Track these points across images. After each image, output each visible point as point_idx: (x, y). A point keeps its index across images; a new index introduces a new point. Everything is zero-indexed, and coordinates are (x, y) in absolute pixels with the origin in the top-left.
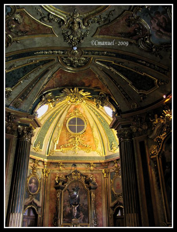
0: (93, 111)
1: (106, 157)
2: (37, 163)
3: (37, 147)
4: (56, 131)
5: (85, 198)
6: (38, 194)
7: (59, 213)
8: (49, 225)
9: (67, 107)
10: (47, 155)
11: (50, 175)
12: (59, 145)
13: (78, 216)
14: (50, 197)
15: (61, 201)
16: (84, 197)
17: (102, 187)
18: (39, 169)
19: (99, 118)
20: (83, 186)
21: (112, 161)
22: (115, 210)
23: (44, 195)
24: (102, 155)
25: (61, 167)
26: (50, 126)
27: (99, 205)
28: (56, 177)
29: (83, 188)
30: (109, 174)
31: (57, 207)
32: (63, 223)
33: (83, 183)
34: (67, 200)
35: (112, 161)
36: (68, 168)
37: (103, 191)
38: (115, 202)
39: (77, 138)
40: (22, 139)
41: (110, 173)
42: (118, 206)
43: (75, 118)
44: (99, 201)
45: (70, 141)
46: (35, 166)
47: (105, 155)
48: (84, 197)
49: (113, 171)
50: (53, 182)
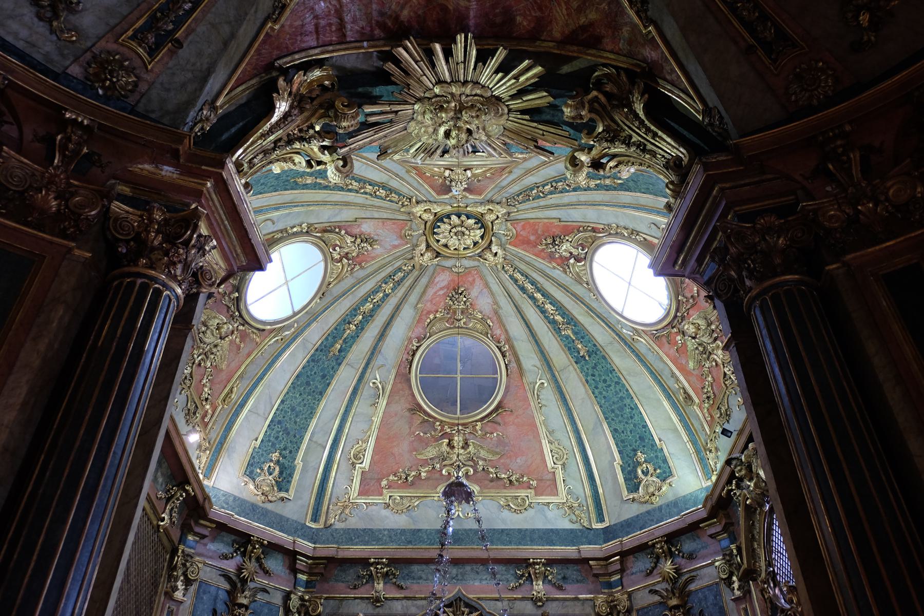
1: (609, 534)
2: (258, 559)
4: (361, 406)
9: (411, 287)
18: (265, 591)
19: (567, 337)
21: (642, 548)
25: (380, 586)
26: (332, 377)
36: (415, 587)
45: (431, 452)
46: (245, 573)
47: (601, 519)
49: (657, 598)
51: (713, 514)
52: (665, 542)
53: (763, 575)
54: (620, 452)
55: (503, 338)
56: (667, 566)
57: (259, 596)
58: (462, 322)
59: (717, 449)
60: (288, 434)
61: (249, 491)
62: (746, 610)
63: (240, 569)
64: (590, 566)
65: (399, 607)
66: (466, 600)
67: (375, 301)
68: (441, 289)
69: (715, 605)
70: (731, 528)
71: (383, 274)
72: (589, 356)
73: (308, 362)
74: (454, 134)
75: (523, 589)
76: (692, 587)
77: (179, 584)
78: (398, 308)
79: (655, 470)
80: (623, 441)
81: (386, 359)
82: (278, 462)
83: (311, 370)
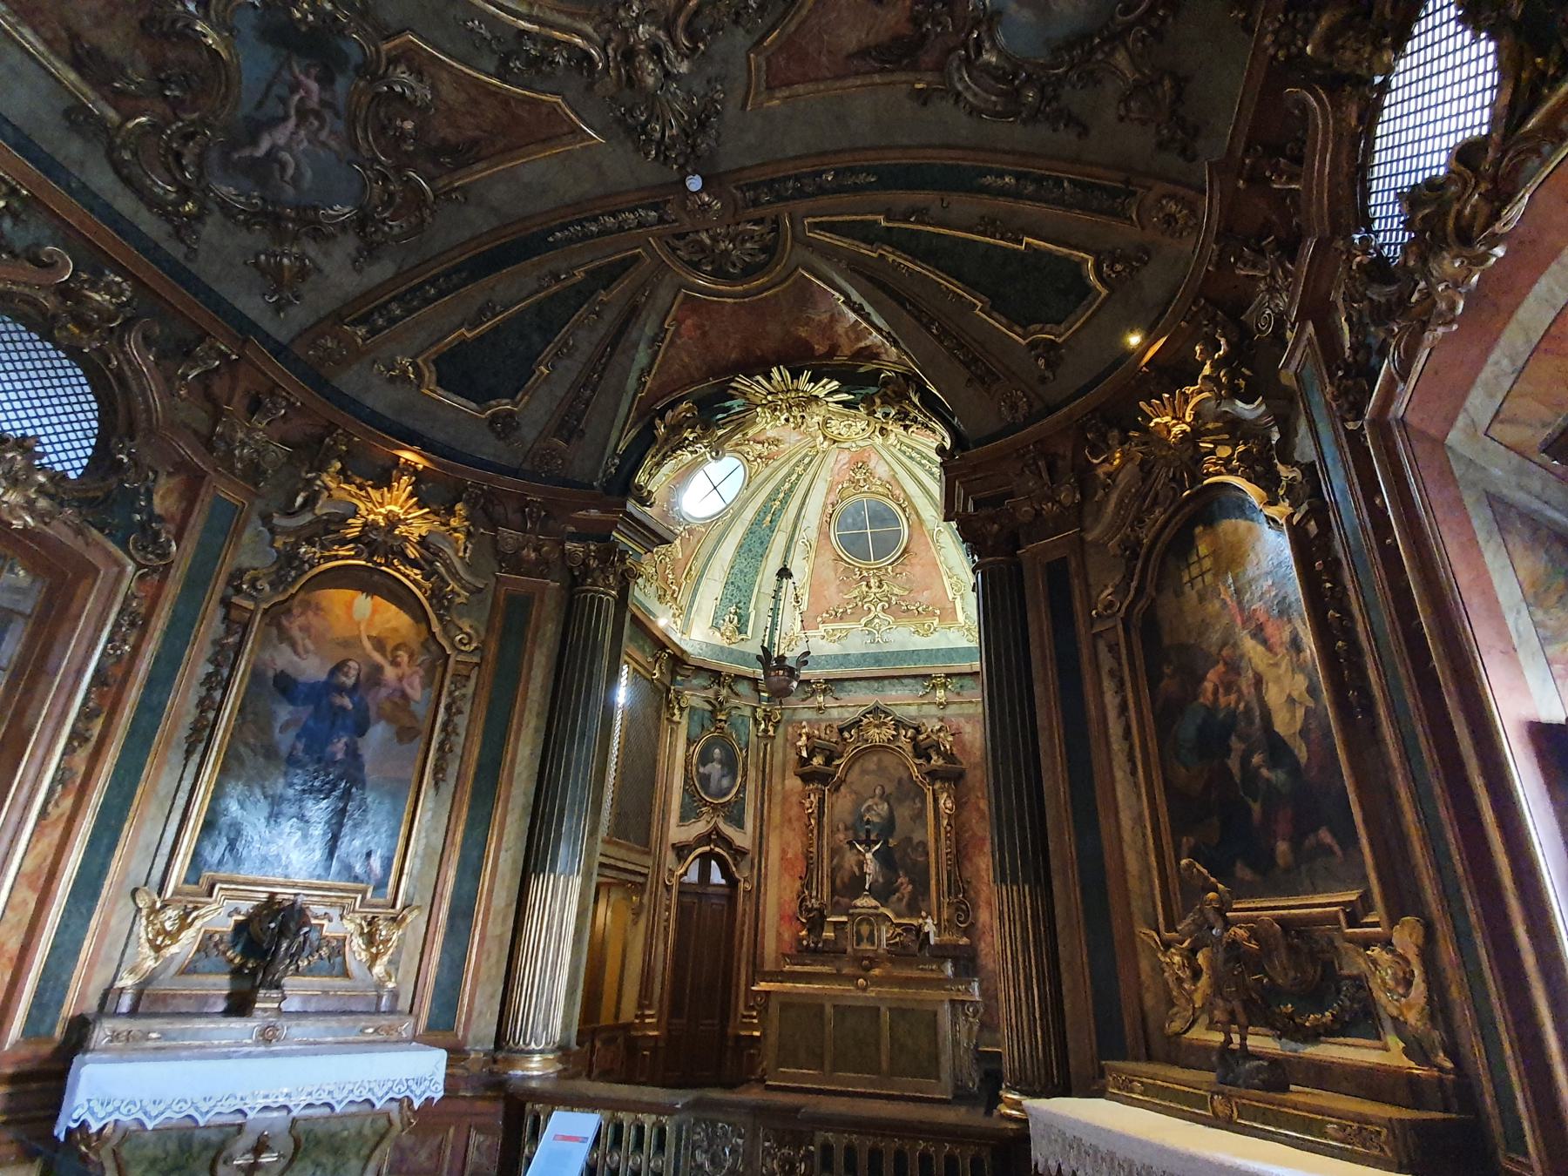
2: (730, 687)
11: (781, 729)
28: (800, 735)
29: (905, 776)
40: (583, 591)
46: (721, 698)
61: (717, 639)
63: (717, 694)
71: (794, 461)
74: (791, 420)
75: (929, 696)
77: (676, 711)
82: (736, 613)
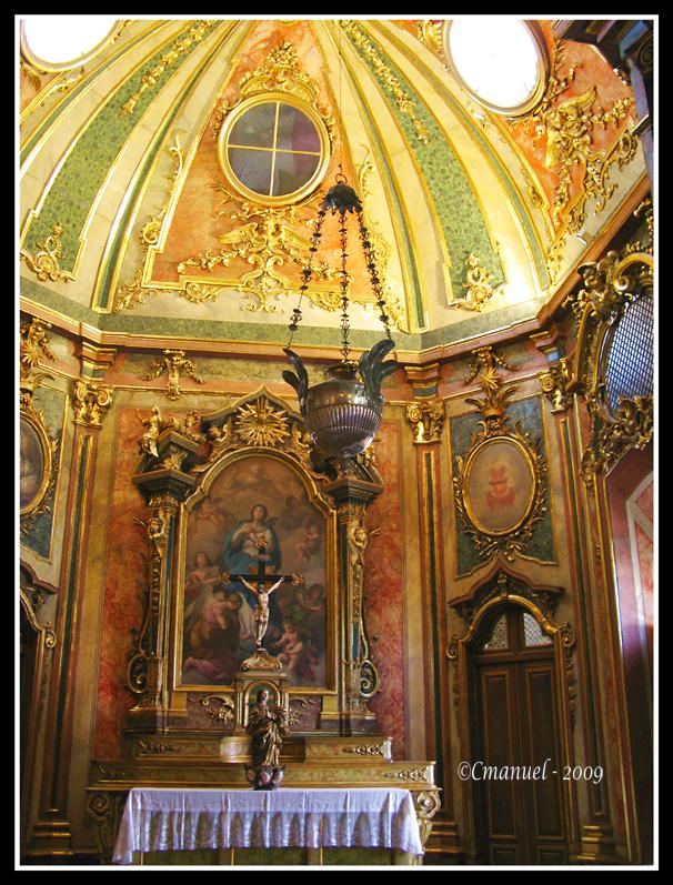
0: (374, 67)
1: (427, 339)
3: (43, 253)
5: (312, 551)
6: (39, 516)
7: (161, 625)
8: (101, 689)
10: (99, 310)
11: (110, 418)
12: (172, 260)
13: (272, 646)
14: (109, 538)
15: (175, 560)
16: (303, 545)
17: (401, 497)
18: (49, 377)
20: (301, 483)
22: (477, 616)
23: (77, 525)
24: (404, 328)
25: (175, 379)
27: (384, 595)
28: (148, 425)
29: (297, 494)
30: (441, 427)
31: (147, 594)
32: (184, 682)
33: (296, 466)
34: (207, 557)
35: (466, 357)
37: (407, 518)
38: (482, 573)
39: (270, 224)
41: (448, 422)
42: (498, 599)
43: (267, 110)
44: (389, 571)
45: (234, 236)
47: (422, 325)
48: (307, 540)
49: (473, 408)
50: (129, 456)
51: (546, 325)
52: (490, 351)
53: (593, 389)
54: (450, 253)
55: (330, 109)
56: (489, 376)
57: (45, 382)
58: (284, 85)
59: (560, 258)
60: (71, 204)
62: (565, 423)
64: (405, 372)
65: (196, 402)
66: (271, 398)
67: (181, 49)
68: (262, 41)
69: (534, 417)
70: (562, 343)
72: (429, 141)
73: (96, 119)
76: (512, 398)
78: (207, 62)
79: (487, 276)
80: (455, 241)
81: (190, 124)
83: (100, 130)
